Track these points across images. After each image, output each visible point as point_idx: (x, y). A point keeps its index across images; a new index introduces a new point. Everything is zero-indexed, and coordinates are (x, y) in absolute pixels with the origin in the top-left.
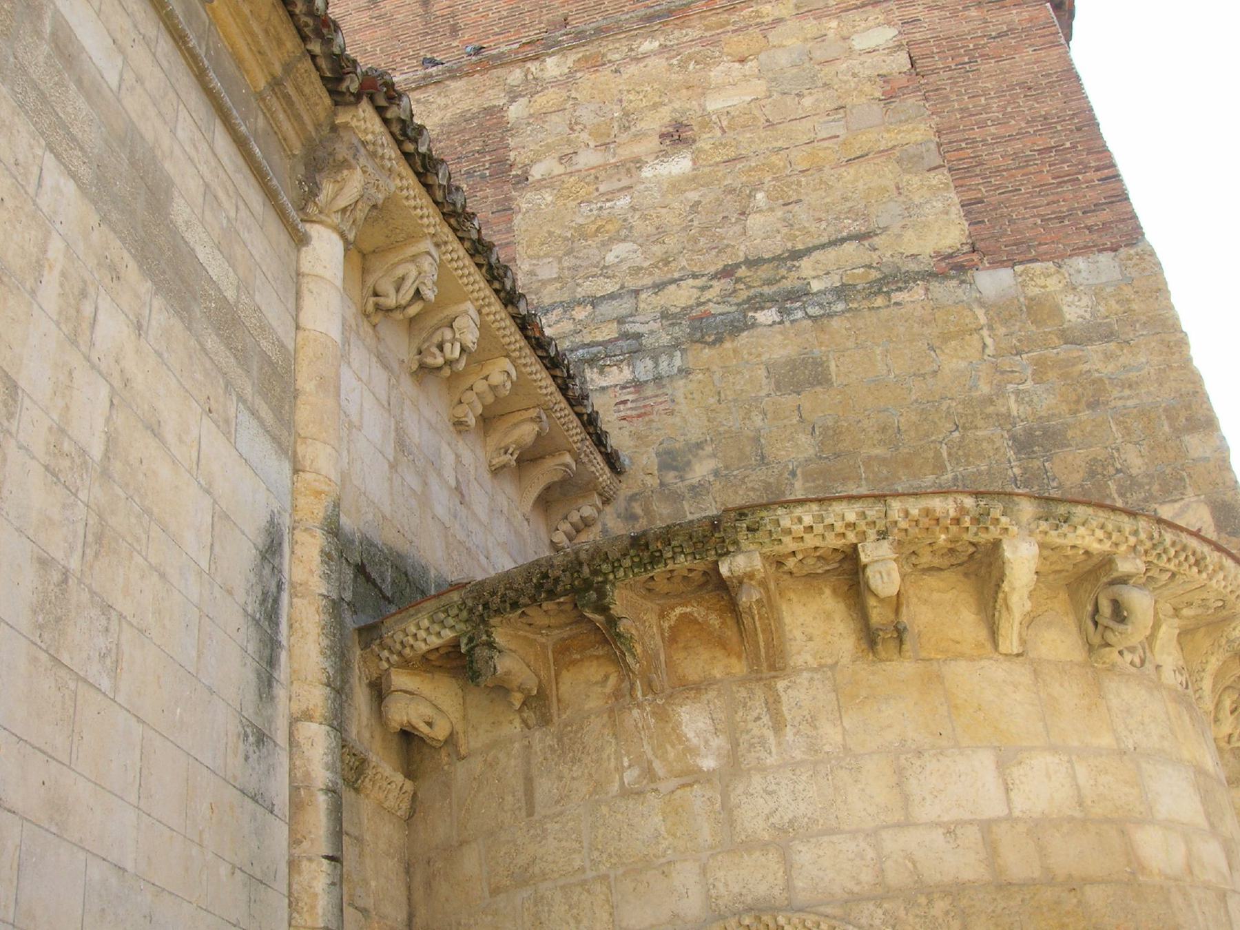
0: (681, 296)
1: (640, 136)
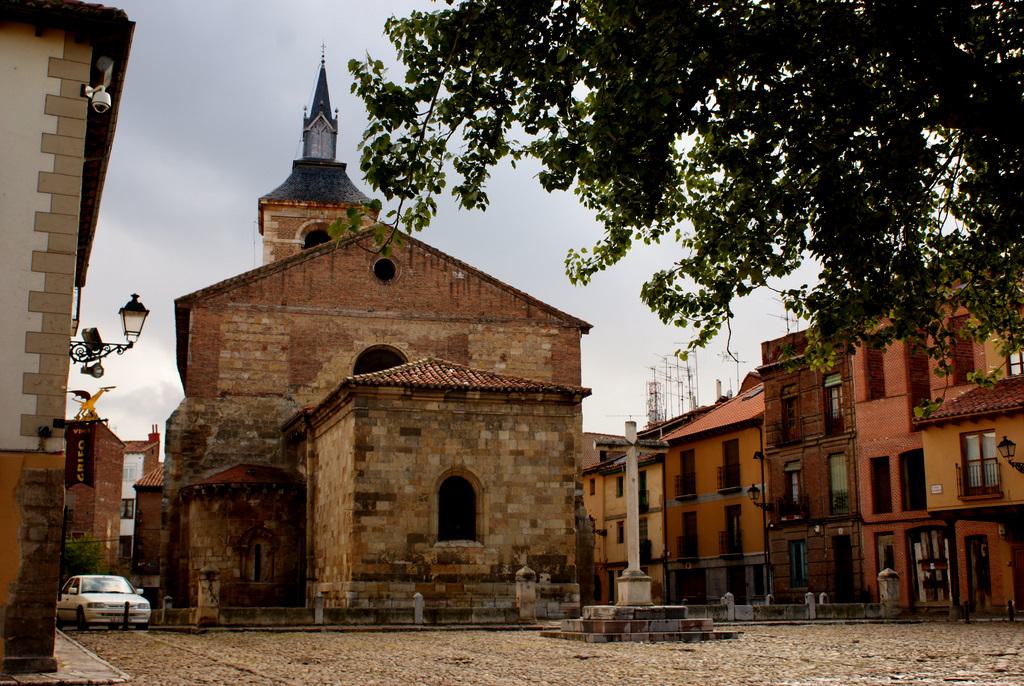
1: (496, 355)
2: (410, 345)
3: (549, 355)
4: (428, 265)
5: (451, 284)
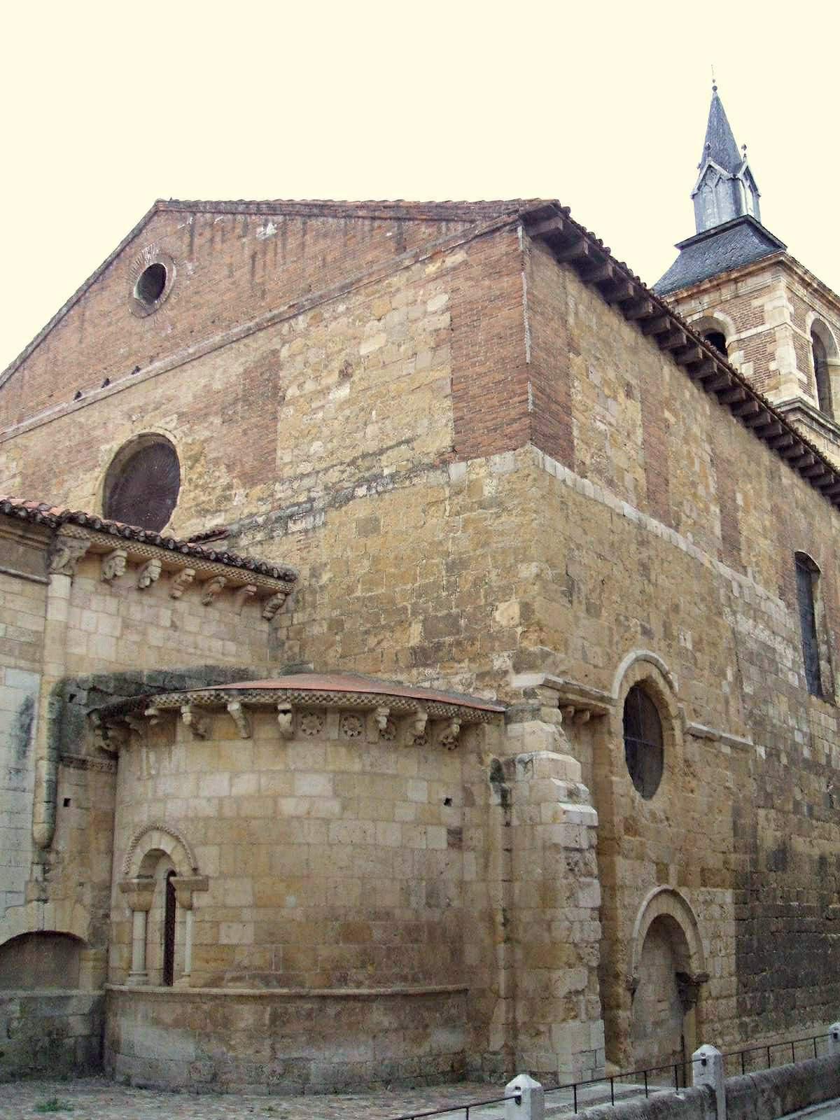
0: (334, 476)
2: (181, 415)
3: (445, 320)
4: (218, 239)
5: (253, 257)
